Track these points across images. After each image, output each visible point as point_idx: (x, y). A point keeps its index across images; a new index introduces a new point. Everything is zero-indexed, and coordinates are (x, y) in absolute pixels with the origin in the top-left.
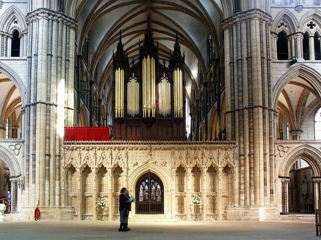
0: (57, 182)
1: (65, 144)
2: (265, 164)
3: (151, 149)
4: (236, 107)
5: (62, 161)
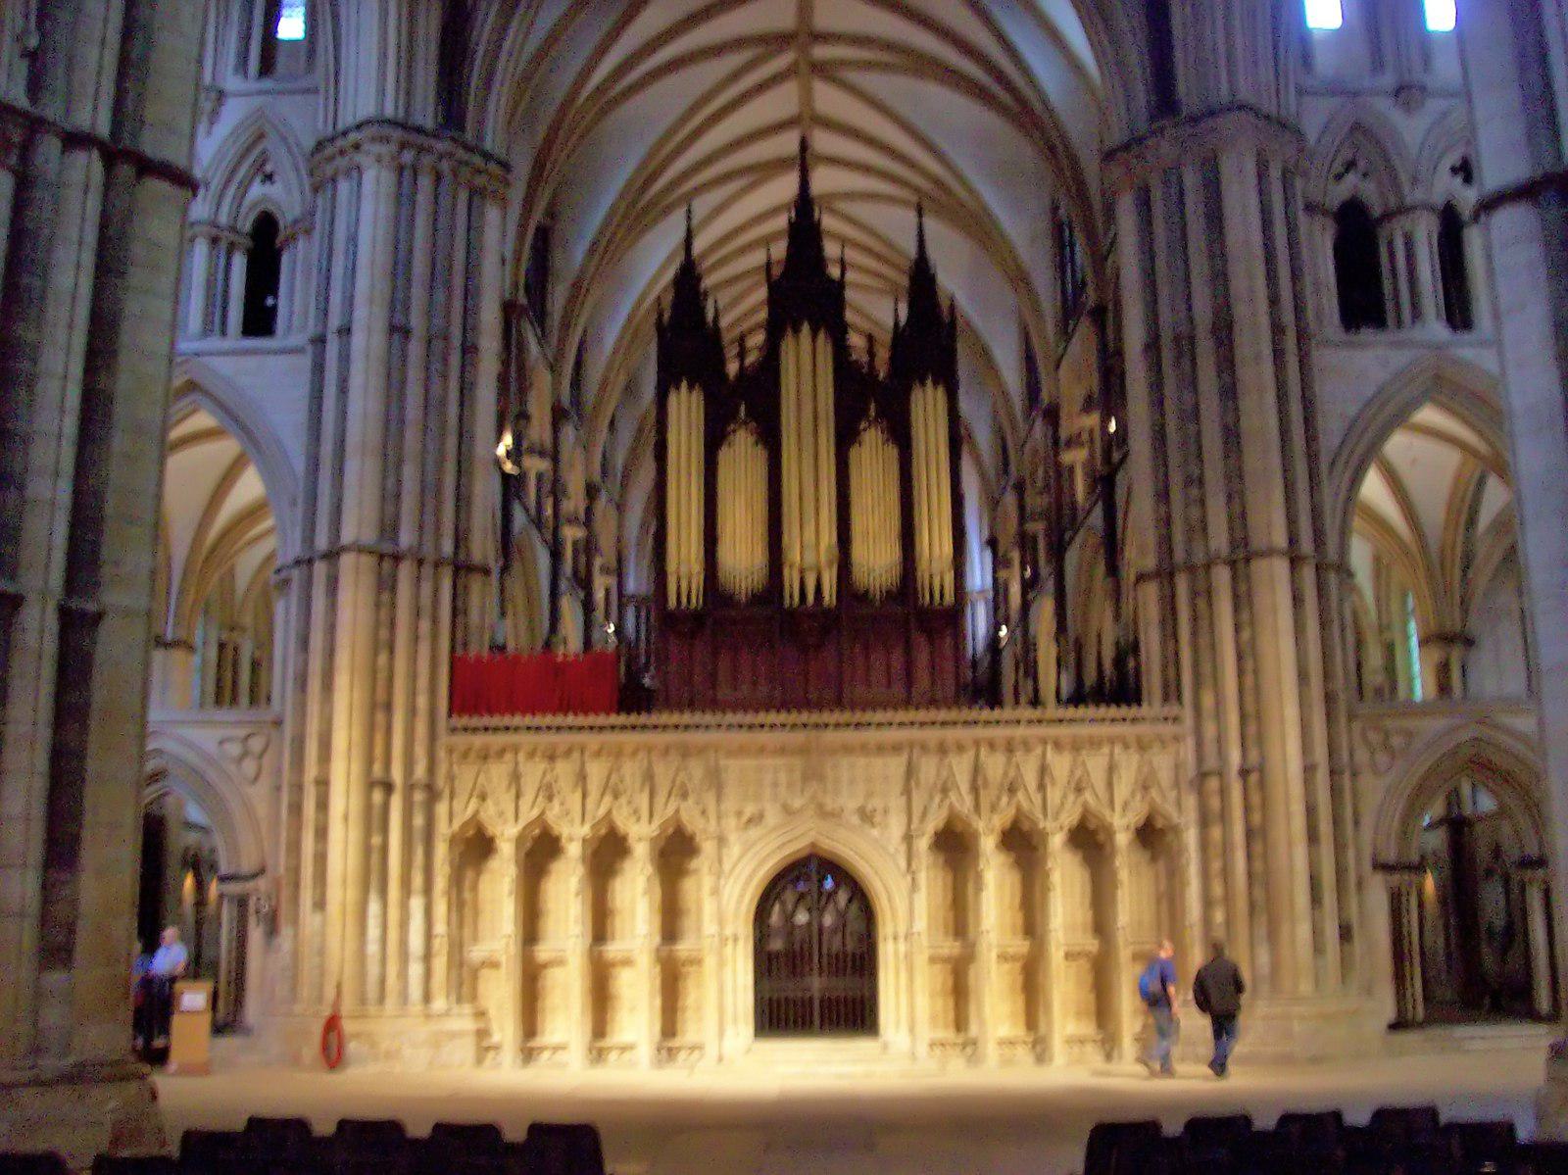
0: (417, 904)
1: (454, 730)
2: (1311, 811)
4: (1179, 555)
5: (442, 809)
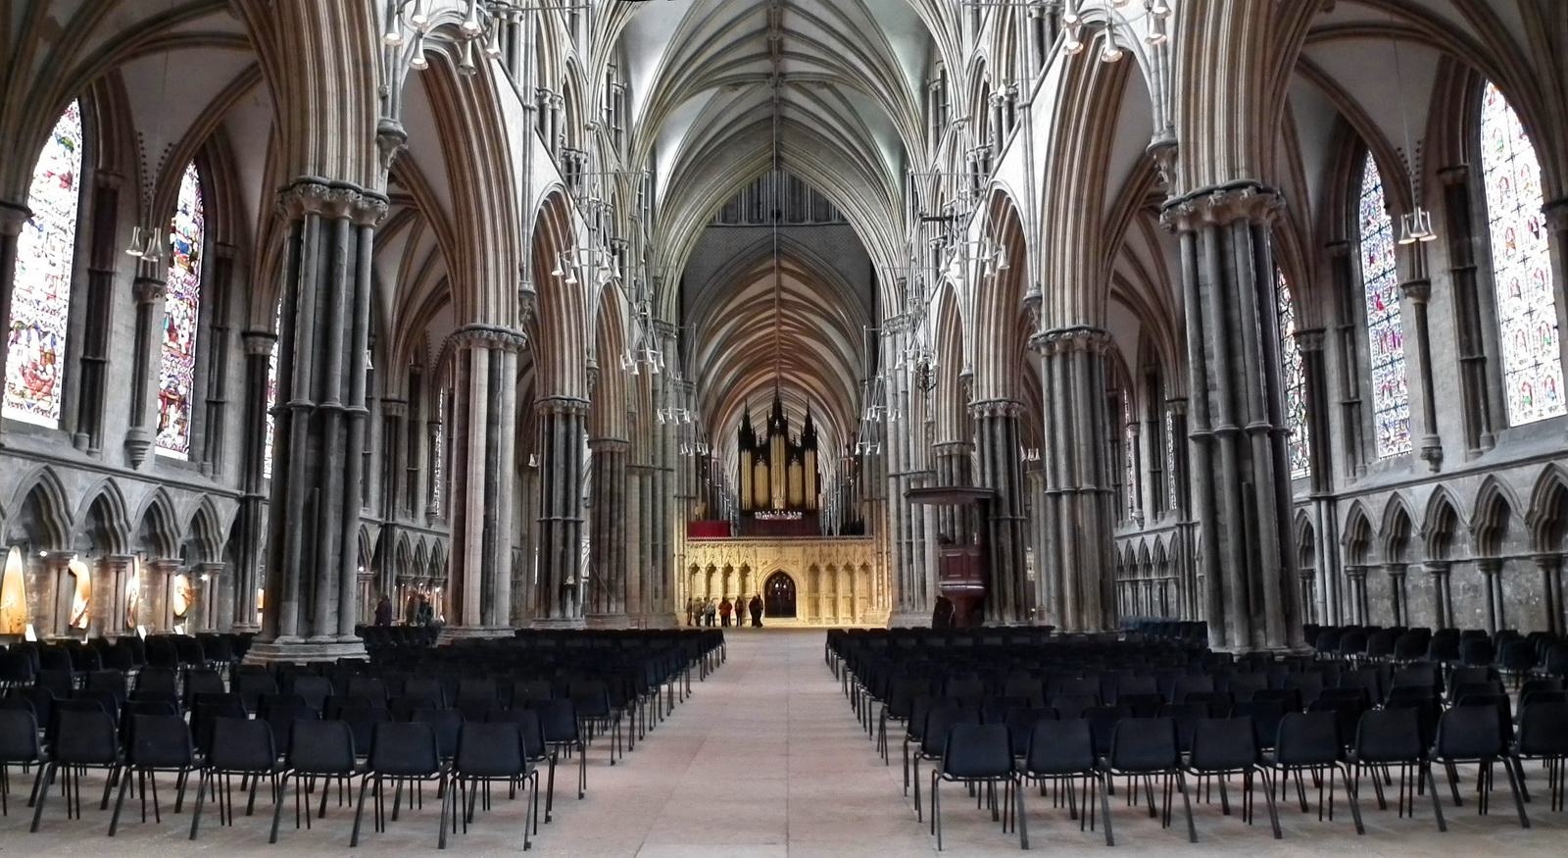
3: (782, 546)
